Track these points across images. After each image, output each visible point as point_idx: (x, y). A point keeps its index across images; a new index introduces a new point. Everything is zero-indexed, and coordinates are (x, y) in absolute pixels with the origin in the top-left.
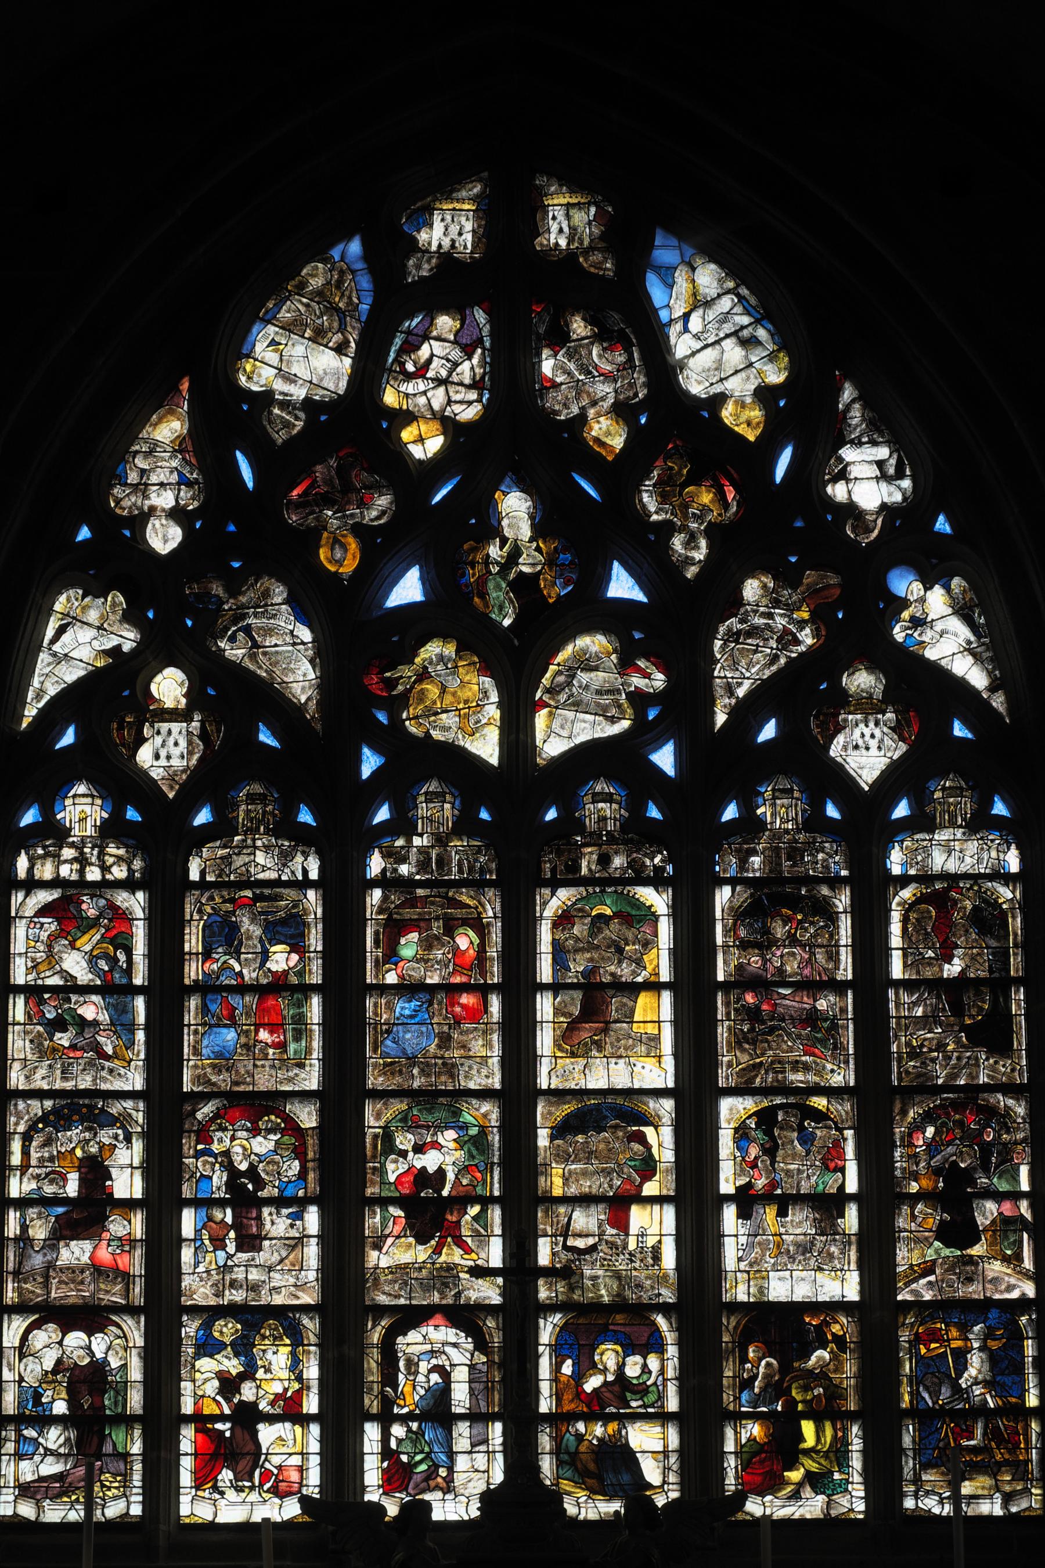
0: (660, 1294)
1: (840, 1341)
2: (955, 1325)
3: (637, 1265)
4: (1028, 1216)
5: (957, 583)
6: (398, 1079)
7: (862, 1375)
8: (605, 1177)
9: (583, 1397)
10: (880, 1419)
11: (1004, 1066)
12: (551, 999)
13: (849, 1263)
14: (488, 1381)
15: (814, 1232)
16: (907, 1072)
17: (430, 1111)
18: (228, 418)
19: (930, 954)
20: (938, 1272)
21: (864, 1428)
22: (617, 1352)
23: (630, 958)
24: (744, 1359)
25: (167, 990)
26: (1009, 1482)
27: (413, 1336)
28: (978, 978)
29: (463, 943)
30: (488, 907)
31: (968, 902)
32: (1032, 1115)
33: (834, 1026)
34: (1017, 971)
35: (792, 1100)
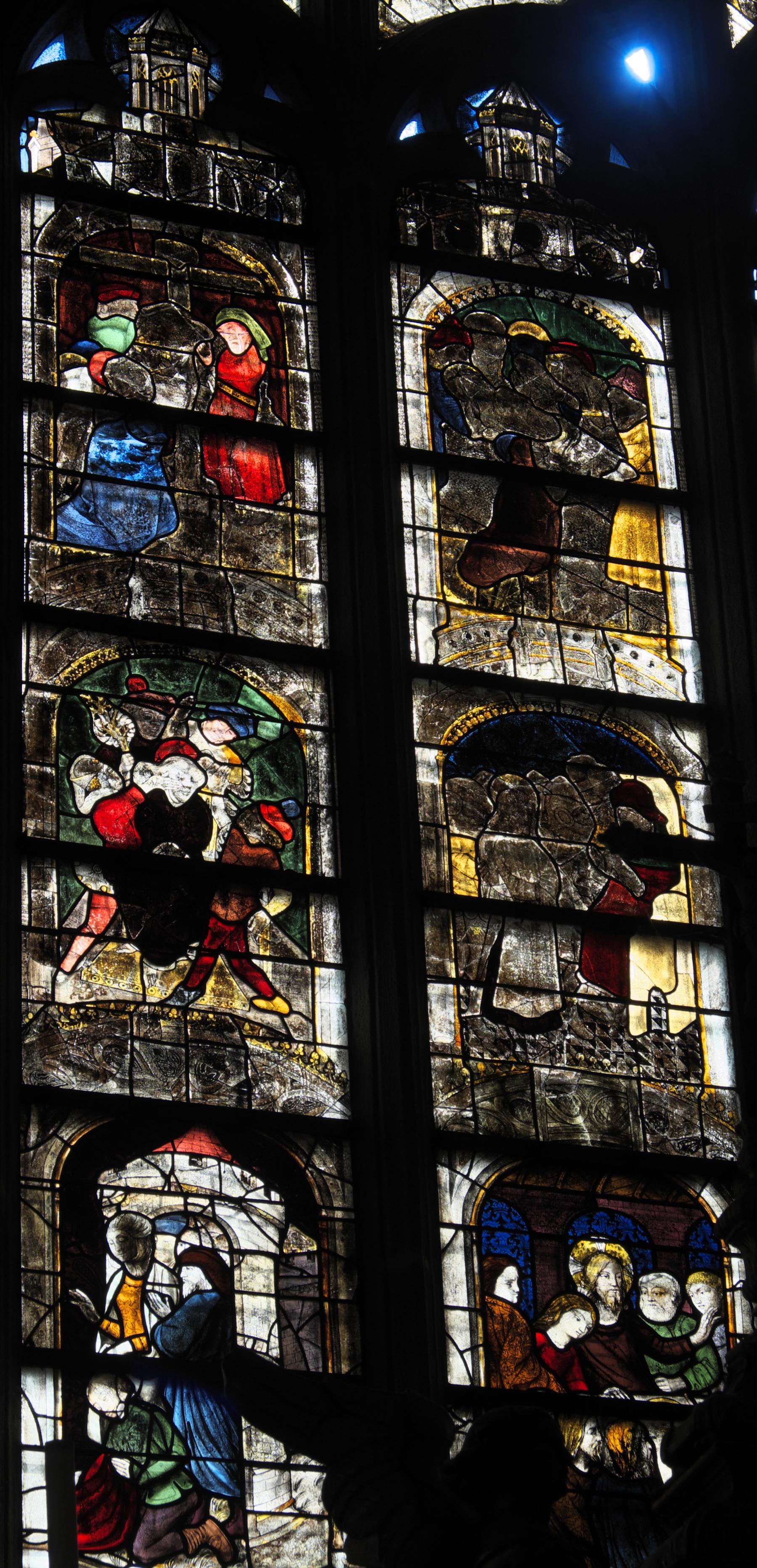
0: (705, 1141)
3: (651, 1069)
6: (96, 595)
8: (569, 871)
9: (547, 1357)
12: (432, 486)
14: (321, 1300)
17: (170, 672)
22: (619, 1261)
23: (593, 433)
27: (139, 1174)
29: (236, 340)
30: (289, 279)
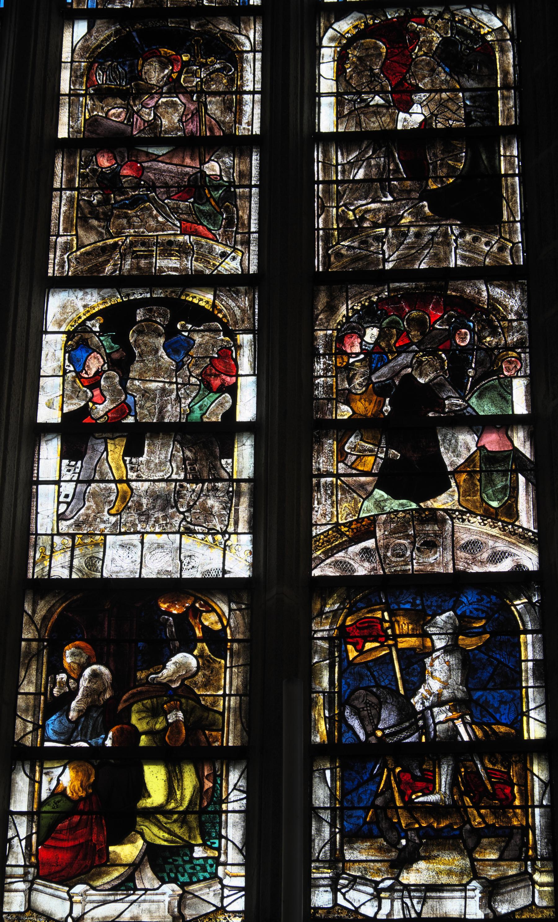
1: (216, 640)
2: (407, 613)
4: (526, 450)
7: (247, 692)
11: (487, 244)
13: (236, 523)
15: (182, 476)
16: (339, 255)
19: (378, 100)
20: (378, 534)
21: (248, 775)
24: (56, 666)
26: (495, 863)
28: (449, 129)
31: (435, 34)
32: (532, 309)
33: (230, 196)
34: (508, 119)
35: (159, 294)
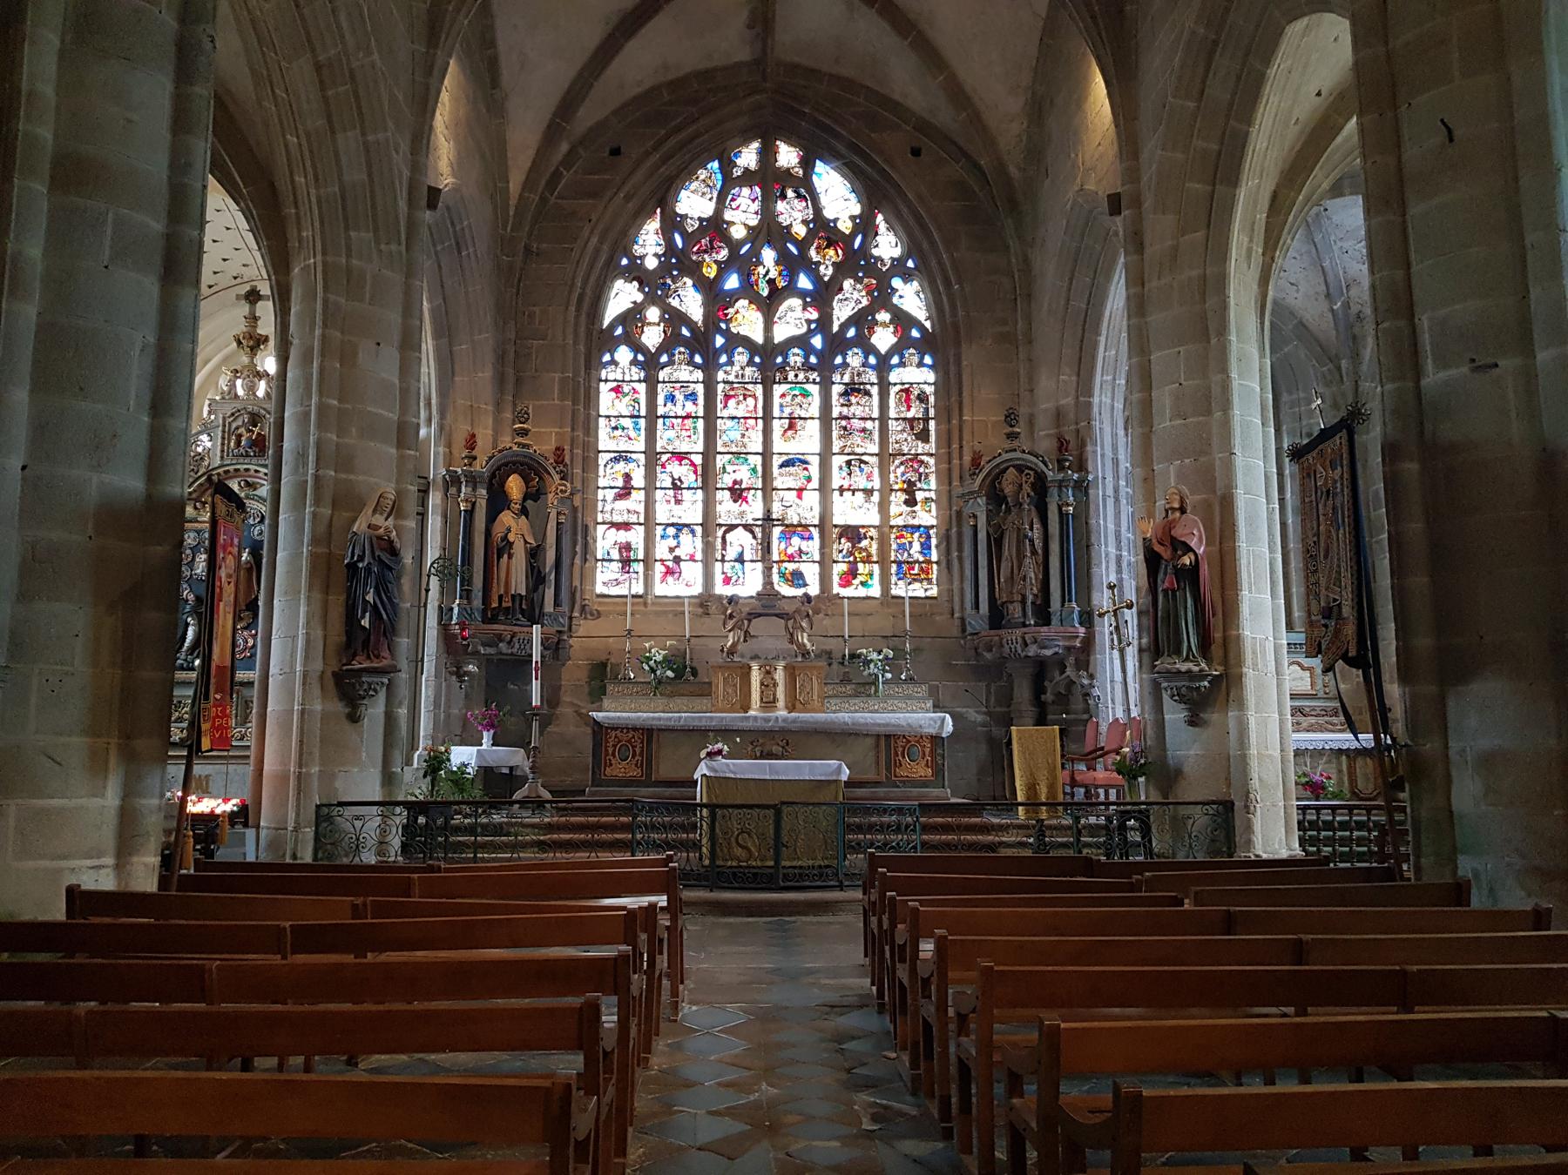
5: (915, 284)
10: (884, 562)
18: (672, 223)
25: (652, 417)
